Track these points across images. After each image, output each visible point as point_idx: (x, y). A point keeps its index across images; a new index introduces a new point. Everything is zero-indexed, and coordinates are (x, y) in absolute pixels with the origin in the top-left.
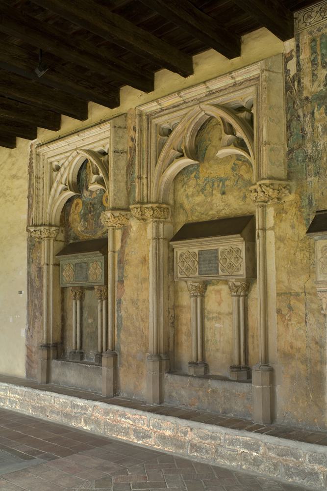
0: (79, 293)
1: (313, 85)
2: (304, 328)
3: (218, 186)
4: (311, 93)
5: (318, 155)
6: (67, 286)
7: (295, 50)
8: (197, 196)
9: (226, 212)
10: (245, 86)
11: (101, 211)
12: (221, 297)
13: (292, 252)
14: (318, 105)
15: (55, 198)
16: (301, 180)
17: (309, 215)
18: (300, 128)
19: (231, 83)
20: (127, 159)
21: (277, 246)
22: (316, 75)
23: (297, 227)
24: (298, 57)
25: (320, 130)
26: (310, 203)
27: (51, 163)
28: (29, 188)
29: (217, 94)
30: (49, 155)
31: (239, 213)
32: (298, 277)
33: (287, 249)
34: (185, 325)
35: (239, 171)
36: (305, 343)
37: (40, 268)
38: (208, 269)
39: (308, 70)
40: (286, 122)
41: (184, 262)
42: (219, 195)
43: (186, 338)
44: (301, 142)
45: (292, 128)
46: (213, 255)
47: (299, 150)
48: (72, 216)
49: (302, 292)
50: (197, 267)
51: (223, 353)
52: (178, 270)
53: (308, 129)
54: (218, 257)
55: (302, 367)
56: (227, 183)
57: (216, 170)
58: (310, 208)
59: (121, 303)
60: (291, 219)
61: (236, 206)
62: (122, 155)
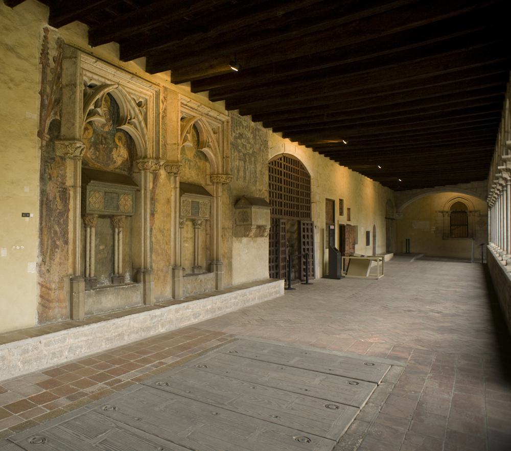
28: (43, 83)
37: (65, 189)
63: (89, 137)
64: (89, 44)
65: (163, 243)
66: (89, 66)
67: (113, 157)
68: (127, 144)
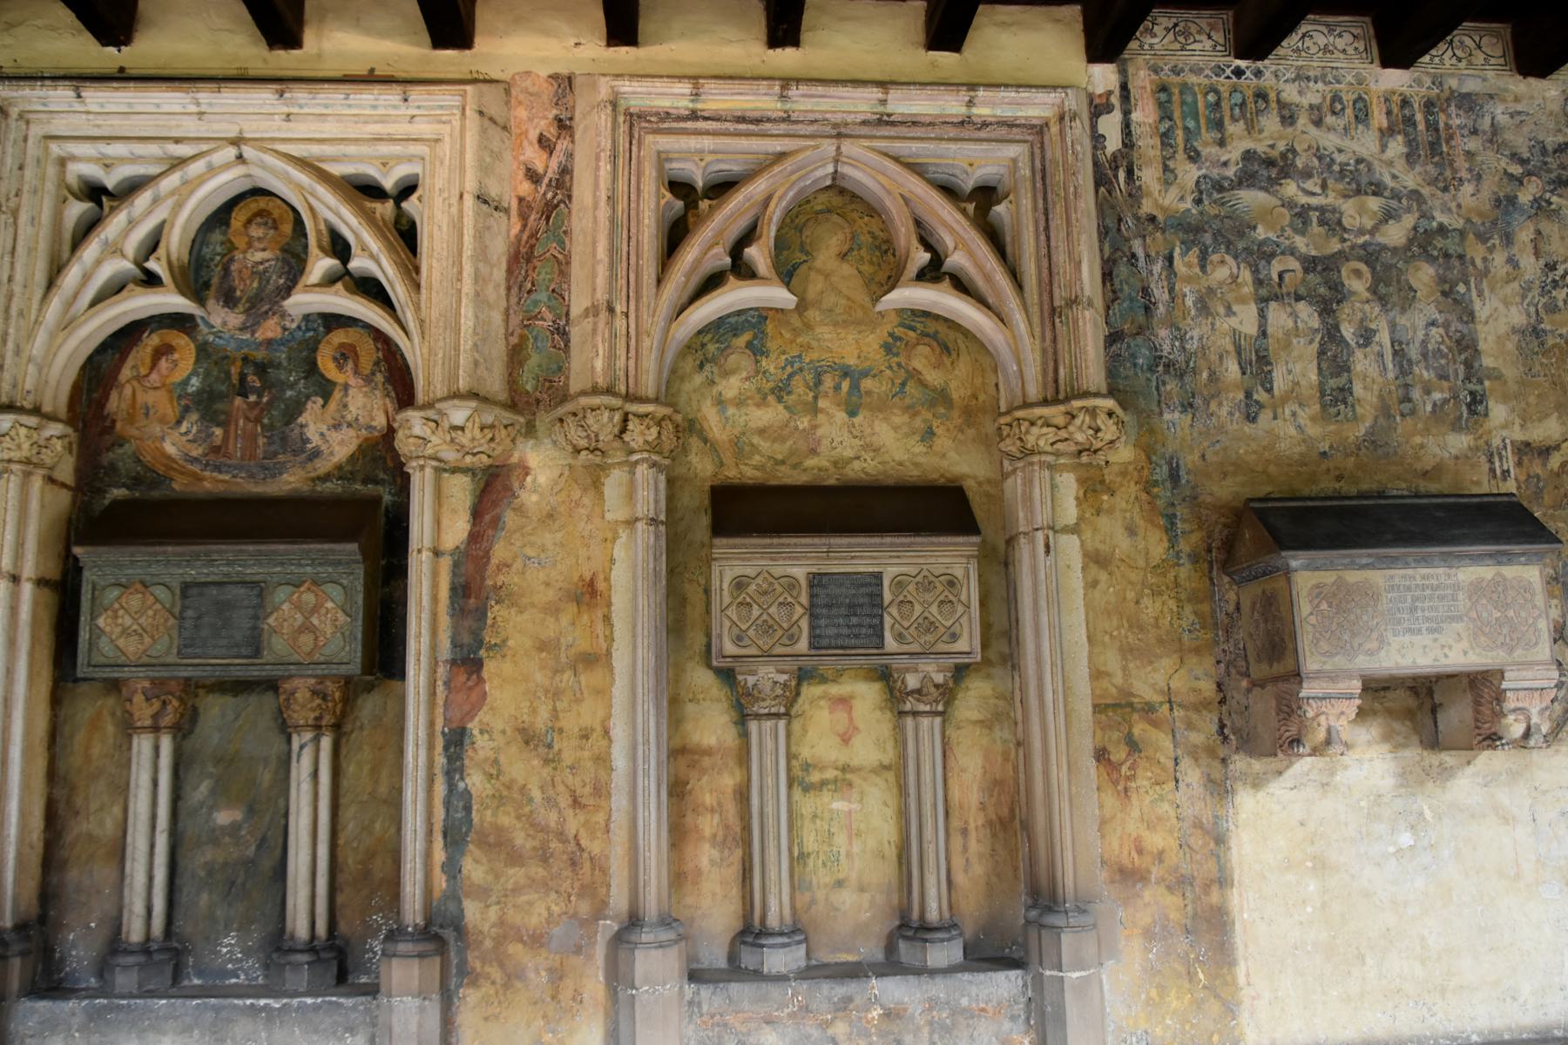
0: (175, 703)
1: (1166, 191)
2: (1170, 797)
3: (837, 388)
4: (1162, 208)
5: (1187, 363)
6: (125, 673)
7: (1117, 92)
8: (758, 406)
9: (864, 468)
10: (993, 135)
11: (308, 397)
12: (851, 719)
13: (1131, 595)
14: (1182, 243)
15: (73, 311)
16: (1149, 416)
17: (1173, 504)
18: (1139, 285)
19: (956, 116)
20: (508, 237)
21: (1090, 580)
22: (1172, 171)
23: (1141, 532)
24: (1126, 113)
25: (1189, 302)
26: (1174, 476)
27: (62, 162)
29: (903, 131)
30: (59, 126)
31: (913, 474)
32: (1151, 663)
33: (1118, 587)
34: (712, 811)
35: (909, 358)
36: (1176, 835)
38: (845, 631)
39: (1152, 153)
40: (1098, 261)
41: (749, 604)
42: (841, 416)
43: (715, 853)
44: (1141, 319)
45: (1117, 281)
46: (863, 590)
47: (1139, 340)
48: (128, 391)
49: (1161, 704)
50: (804, 624)
51: (862, 889)
52: (726, 630)
53: (1160, 293)
54: (881, 596)
55: (1171, 901)
56: (867, 384)
57: (831, 340)
58: (1173, 488)
59: (467, 741)
60: (1125, 511)
61: (900, 455)
62: (496, 214)
63: (178, 377)
64: (105, 44)
65: (550, 802)
66: (74, 119)
67: (302, 434)
68: (390, 369)
